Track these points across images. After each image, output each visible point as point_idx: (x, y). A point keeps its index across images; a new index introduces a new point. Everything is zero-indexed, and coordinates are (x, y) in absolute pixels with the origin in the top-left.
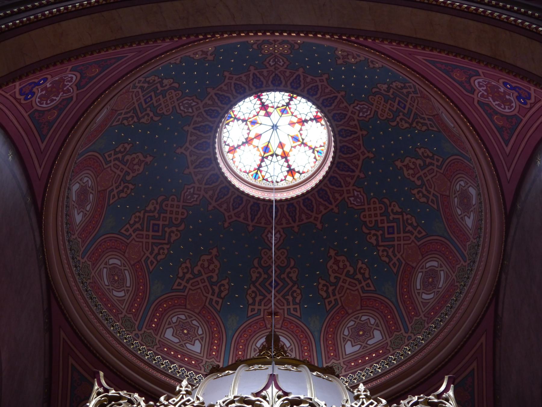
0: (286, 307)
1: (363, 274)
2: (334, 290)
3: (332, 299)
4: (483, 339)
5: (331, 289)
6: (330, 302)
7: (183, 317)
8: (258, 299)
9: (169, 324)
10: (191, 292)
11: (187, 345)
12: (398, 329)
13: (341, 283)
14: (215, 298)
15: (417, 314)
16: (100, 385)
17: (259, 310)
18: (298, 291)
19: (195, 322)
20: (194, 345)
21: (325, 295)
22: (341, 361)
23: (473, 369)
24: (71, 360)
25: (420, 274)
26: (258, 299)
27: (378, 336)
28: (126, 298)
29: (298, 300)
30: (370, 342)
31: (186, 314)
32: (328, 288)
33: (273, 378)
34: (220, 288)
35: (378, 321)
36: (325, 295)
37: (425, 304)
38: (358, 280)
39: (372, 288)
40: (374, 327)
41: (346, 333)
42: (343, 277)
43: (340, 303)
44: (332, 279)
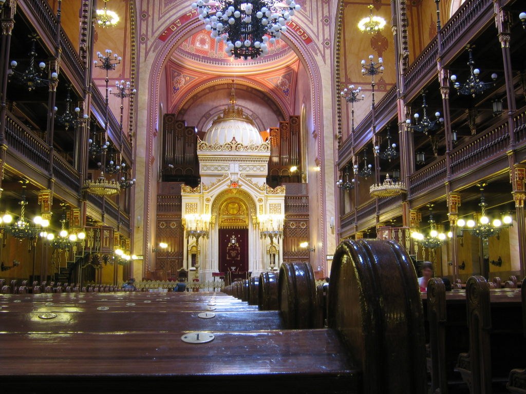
33: (234, 138)
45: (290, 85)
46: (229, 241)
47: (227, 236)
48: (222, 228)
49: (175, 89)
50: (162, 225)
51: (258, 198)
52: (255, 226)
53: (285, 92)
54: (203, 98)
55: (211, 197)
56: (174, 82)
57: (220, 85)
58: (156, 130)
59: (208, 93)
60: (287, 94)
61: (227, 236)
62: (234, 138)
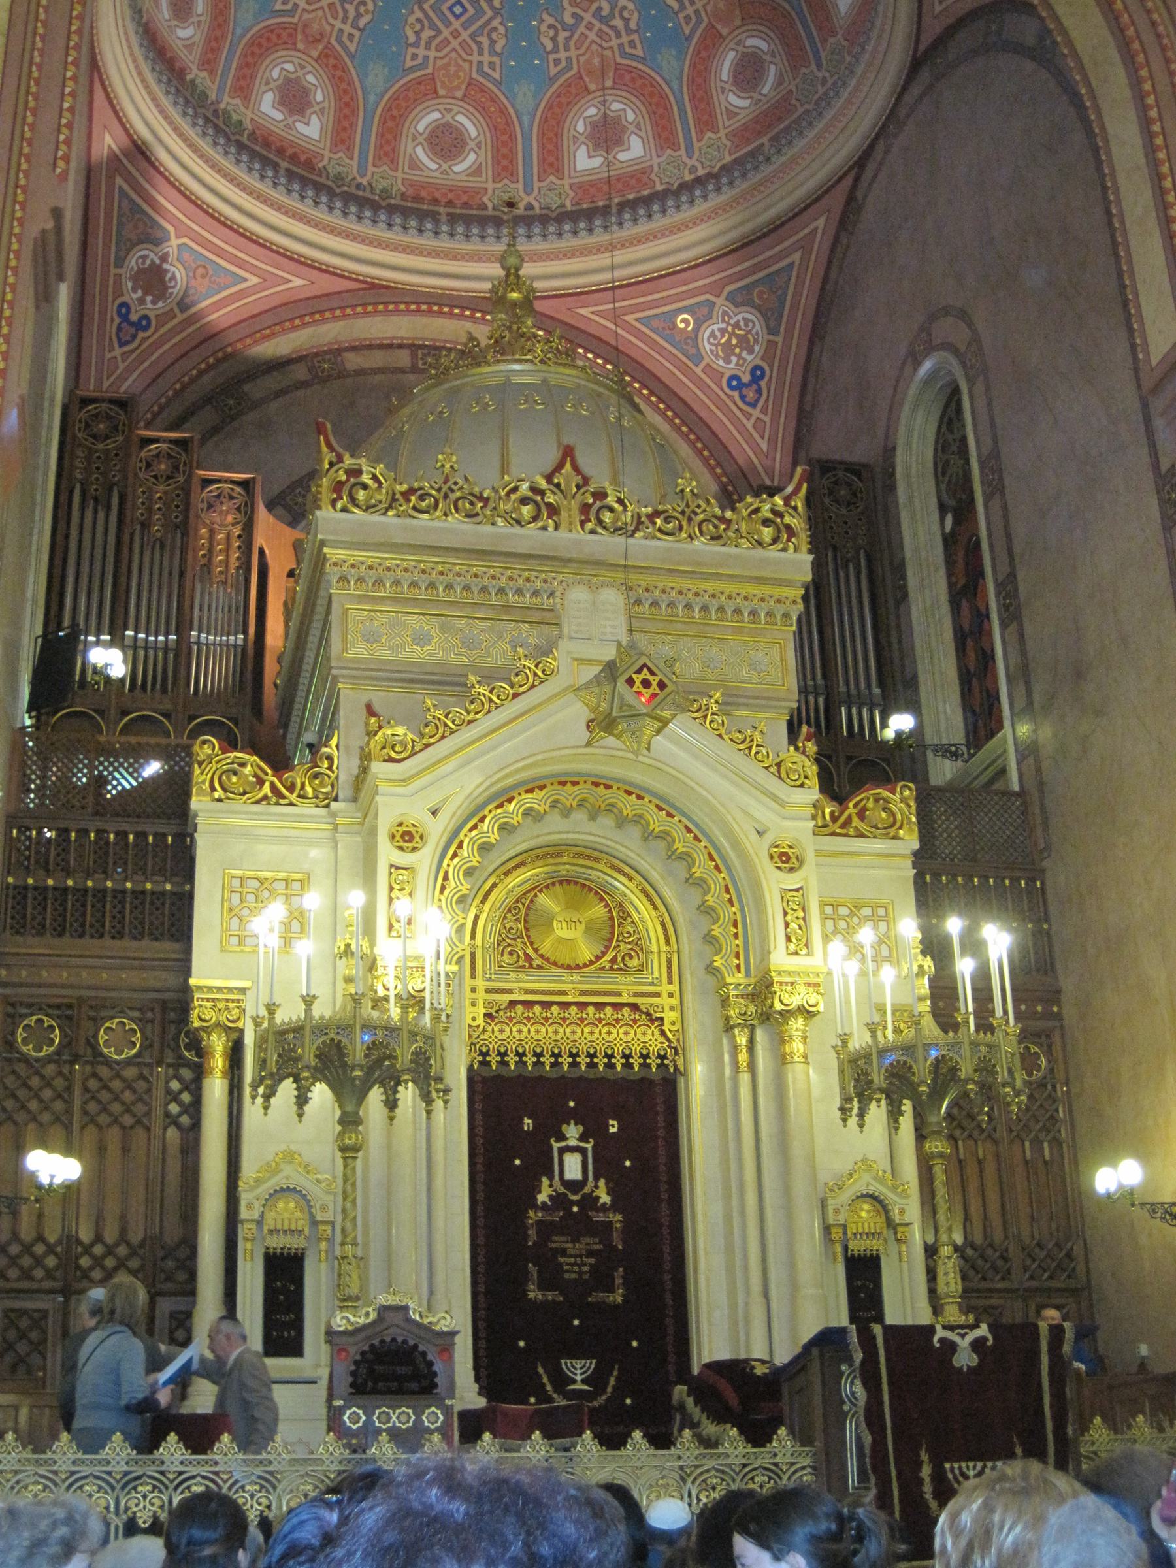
0: (475, 58)
1: (626, 21)
2: (568, 39)
3: (562, 55)
4: (821, 222)
5: (563, 35)
6: (557, 62)
7: (289, 67)
8: (427, 34)
9: (267, 83)
10: (306, 16)
11: (298, 125)
12: (675, 146)
13: (582, 28)
14: (347, 29)
15: (714, 129)
16: (331, 448)
17: (426, 58)
18: (502, 30)
19: (310, 78)
20: (307, 124)
21: (549, 45)
22: (566, 182)
23: (793, 263)
24: (119, 181)
25: (732, 54)
26: (427, 34)
27: (635, 150)
28: (197, 38)
29: (498, 48)
30: (622, 156)
31: (296, 61)
32: (556, 34)
33: (568, 453)
34: (357, 9)
35: (640, 118)
36: (549, 45)
37: (731, 114)
38: (613, 28)
39: (639, 52)
40: (632, 128)
41: (580, 127)
42: (588, 17)
43: (575, 67)
44: (569, 20)
45: (771, 345)
46: (544, 1164)
47: (527, 1121)
48: (494, 1060)
49: (125, 318)
50: (40, 1036)
51: (769, 838)
52: (742, 1040)
53: (741, 386)
54: (274, 406)
55: (434, 813)
56: (121, 271)
57: (370, 347)
58: (57, 214)
59: (304, 384)
60: (751, 394)
61: (528, 1123)
62: (568, 453)
